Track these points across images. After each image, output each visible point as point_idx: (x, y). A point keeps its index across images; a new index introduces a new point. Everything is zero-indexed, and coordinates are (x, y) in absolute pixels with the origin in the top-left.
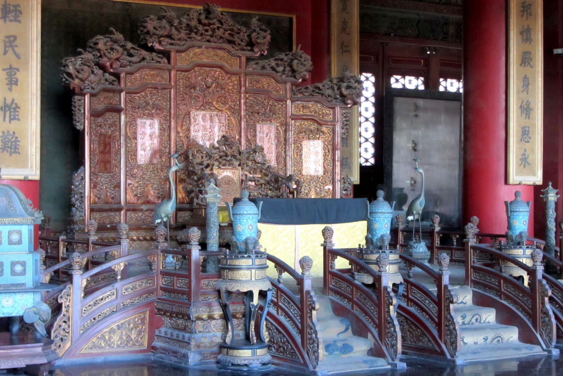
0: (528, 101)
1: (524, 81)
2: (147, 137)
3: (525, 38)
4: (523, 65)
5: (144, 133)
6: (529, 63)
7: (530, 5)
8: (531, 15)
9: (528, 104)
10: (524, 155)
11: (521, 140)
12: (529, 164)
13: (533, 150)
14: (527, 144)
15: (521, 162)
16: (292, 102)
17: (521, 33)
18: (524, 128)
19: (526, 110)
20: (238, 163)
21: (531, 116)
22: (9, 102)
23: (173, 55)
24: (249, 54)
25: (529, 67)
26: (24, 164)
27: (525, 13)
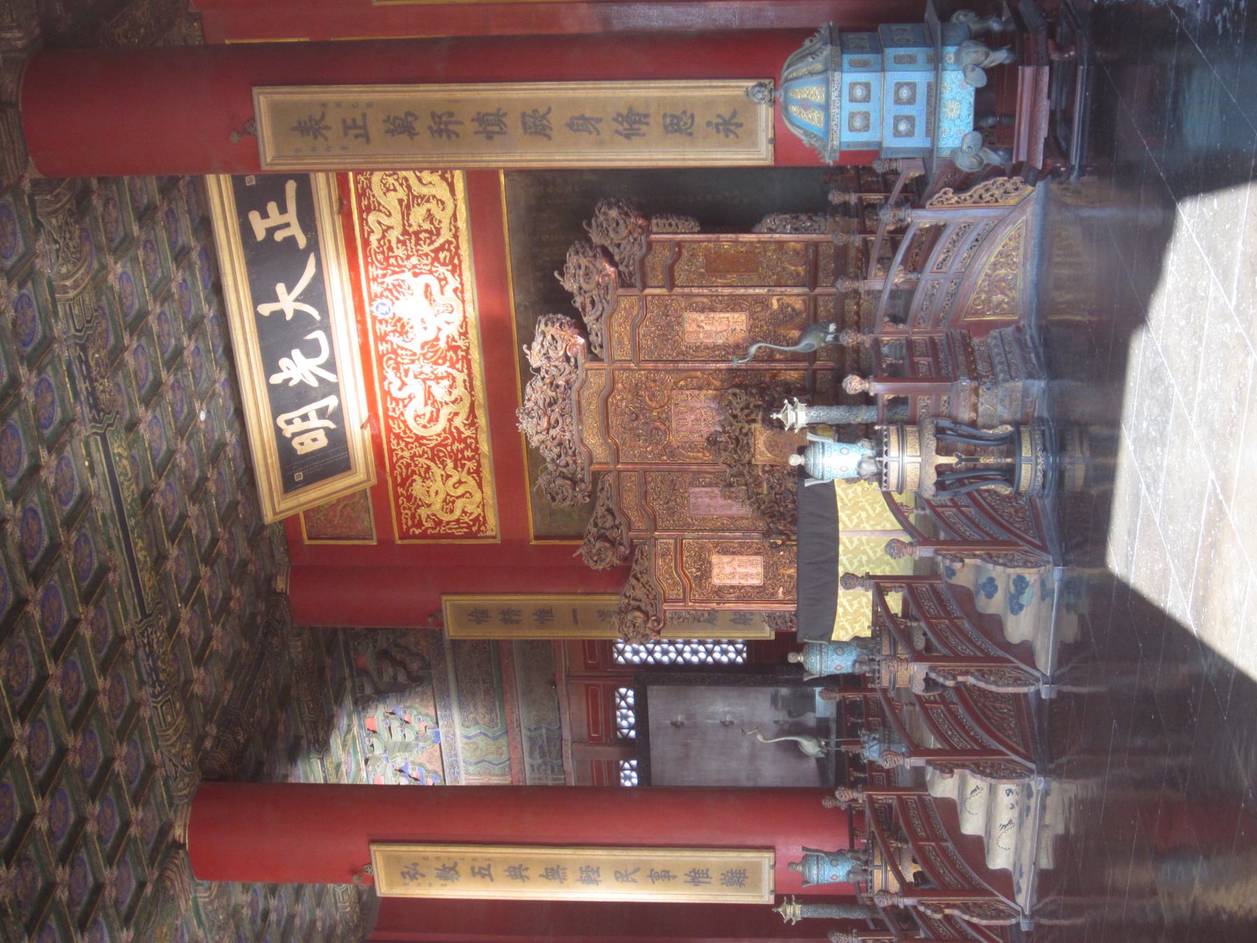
0: (615, 119)
1: (578, 130)
2: (713, 502)
3: (496, 129)
4: (547, 132)
5: (709, 506)
6: (544, 117)
7: (433, 115)
8: (451, 114)
9: (619, 118)
10: (717, 126)
11: (691, 134)
12: (734, 114)
13: (709, 103)
14: (697, 119)
15: (731, 136)
16: (645, 286)
17: (490, 137)
18: (666, 127)
19: (632, 123)
20: (747, 426)
21: (642, 111)
22: (689, 879)
23: (595, 467)
24: (581, 360)
25: (550, 116)
26: (757, 866)
27: (451, 127)
